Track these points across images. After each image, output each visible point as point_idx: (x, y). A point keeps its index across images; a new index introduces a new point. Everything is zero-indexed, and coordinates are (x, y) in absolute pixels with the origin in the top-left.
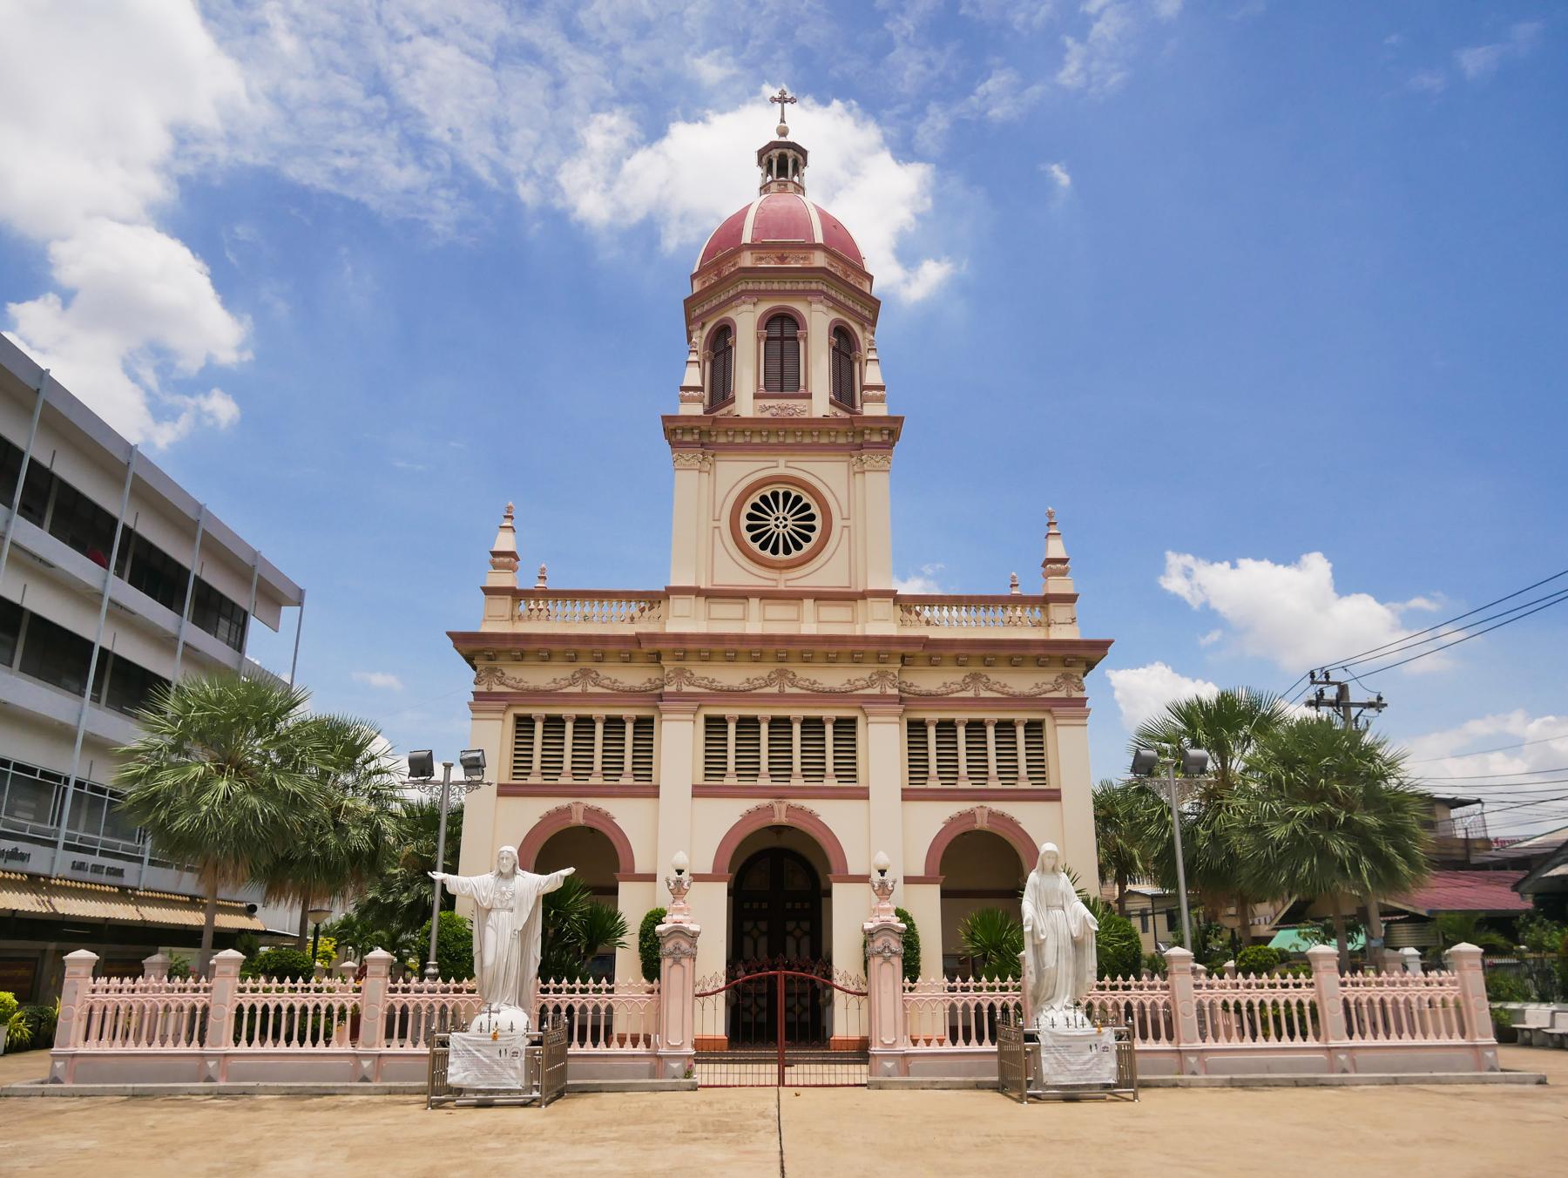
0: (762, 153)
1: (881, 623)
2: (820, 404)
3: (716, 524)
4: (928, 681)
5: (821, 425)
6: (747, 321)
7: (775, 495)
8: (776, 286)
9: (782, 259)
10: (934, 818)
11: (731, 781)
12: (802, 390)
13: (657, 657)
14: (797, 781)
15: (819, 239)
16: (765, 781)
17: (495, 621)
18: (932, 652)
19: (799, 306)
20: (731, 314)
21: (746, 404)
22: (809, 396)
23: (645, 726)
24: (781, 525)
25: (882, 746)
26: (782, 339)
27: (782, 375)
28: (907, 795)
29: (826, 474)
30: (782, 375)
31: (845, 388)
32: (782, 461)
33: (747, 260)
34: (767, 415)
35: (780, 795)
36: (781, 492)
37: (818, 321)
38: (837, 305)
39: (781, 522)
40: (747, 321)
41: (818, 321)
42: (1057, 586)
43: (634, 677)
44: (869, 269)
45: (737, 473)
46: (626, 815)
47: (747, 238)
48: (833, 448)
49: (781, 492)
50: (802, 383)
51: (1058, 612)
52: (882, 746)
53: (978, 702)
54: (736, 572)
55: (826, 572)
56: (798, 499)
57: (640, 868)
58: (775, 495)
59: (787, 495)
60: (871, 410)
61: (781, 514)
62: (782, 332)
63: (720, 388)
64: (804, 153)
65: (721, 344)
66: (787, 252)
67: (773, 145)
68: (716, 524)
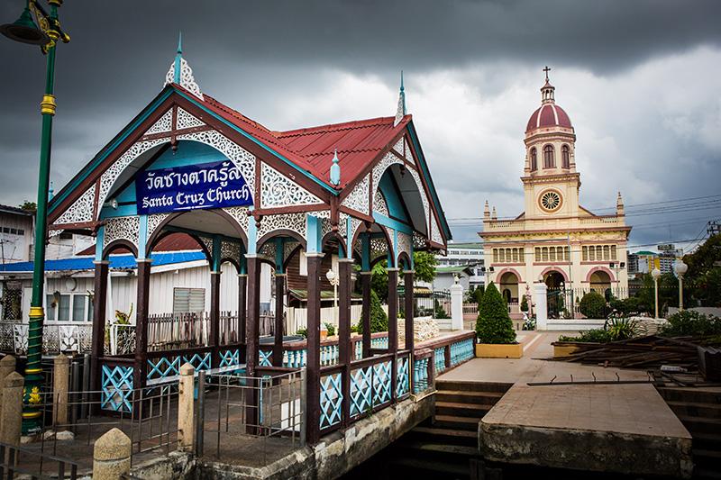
0: (541, 90)
1: (576, 224)
2: (559, 170)
4: (586, 237)
5: (559, 176)
6: (540, 148)
10: (589, 268)
11: (541, 262)
13: (523, 235)
14: (556, 261)
15: (557, 123)
16: (549, 261)
17: (487, 229)
18: (587, 231)
19: (552, 143)
21: (541, 172)
23: (522, 249)
24: (551, 201)
25: (576, 255)
26: (549, 152)
27: (549, 164)
28: (581, 263)
29: (560, 188)
30: (549, 164)
31: (566, 164)
33: (539, 132)
34: (546, 174)
35: (553, 264)
37: (558, 146)
38: (563, 140)
39: (551, 201)
40: (540, 148)
41: (558, 146)
42: (620, 212)
43: (520, 239)
44: (573, 125)
45: (540, 189)
46: (518, 269)
47: (538, 126)
48: (562, 181)
51: (620, 219)
52: (576, 255)
53: (599, 242)
54: (540, 213)
55: (562, 212)
57: (523, 281)
60: (571, 171)
62: (549, 150)
63: (534, 168)
64: (554, 88)
67: (544, 88)
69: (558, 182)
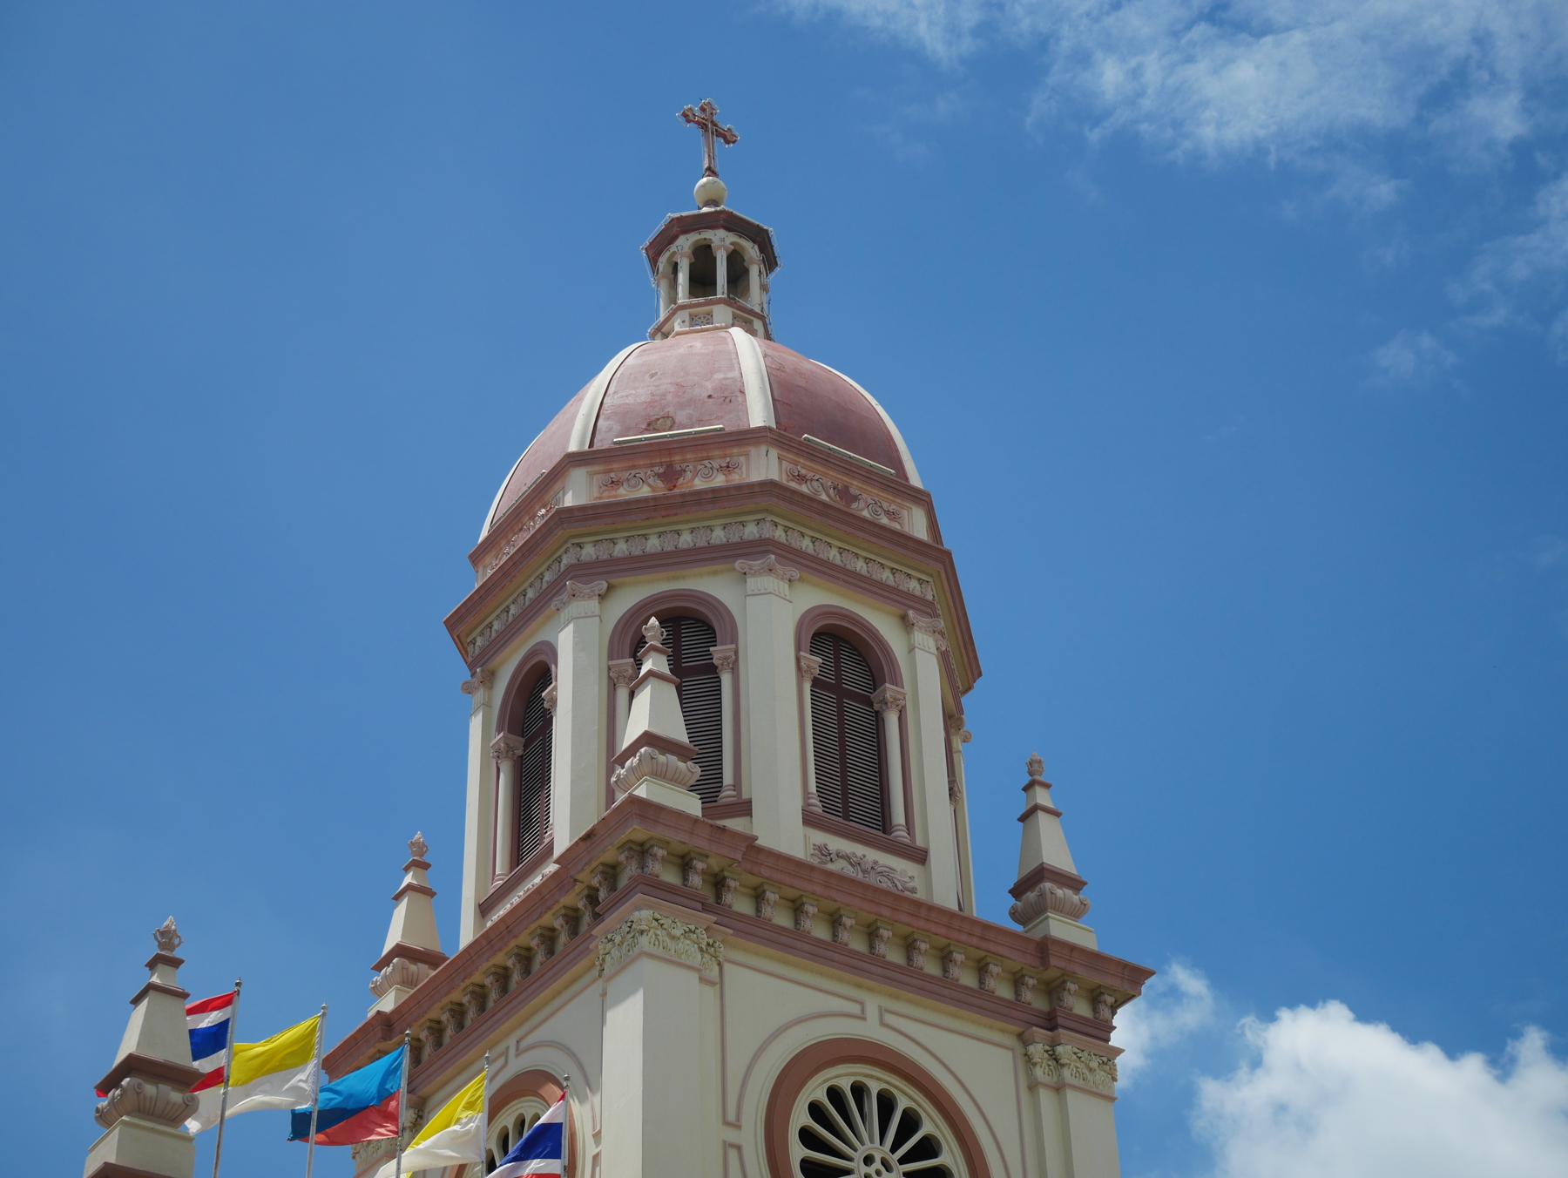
3: (731, 1135)
6: (768, 622)
7: (859, 1091)
8: (833, 555)
9: (845, 494)
12: (901, 834)
20: (714, 586)
22: (920, 856)
29: (971, 1064)
32: (873, 1003)
36: (874, 1088)
48: (977, 1002)
49: (874, 1088)
50: (898, 817)
56: (910, 1123)
58: (859, 1091)
59: (886, 1104)
61: (881, 1151)
62: (846, 671)
65: (693, 645)
66: (856, 486)
68: (731, 1135)
69: (941, 991)
